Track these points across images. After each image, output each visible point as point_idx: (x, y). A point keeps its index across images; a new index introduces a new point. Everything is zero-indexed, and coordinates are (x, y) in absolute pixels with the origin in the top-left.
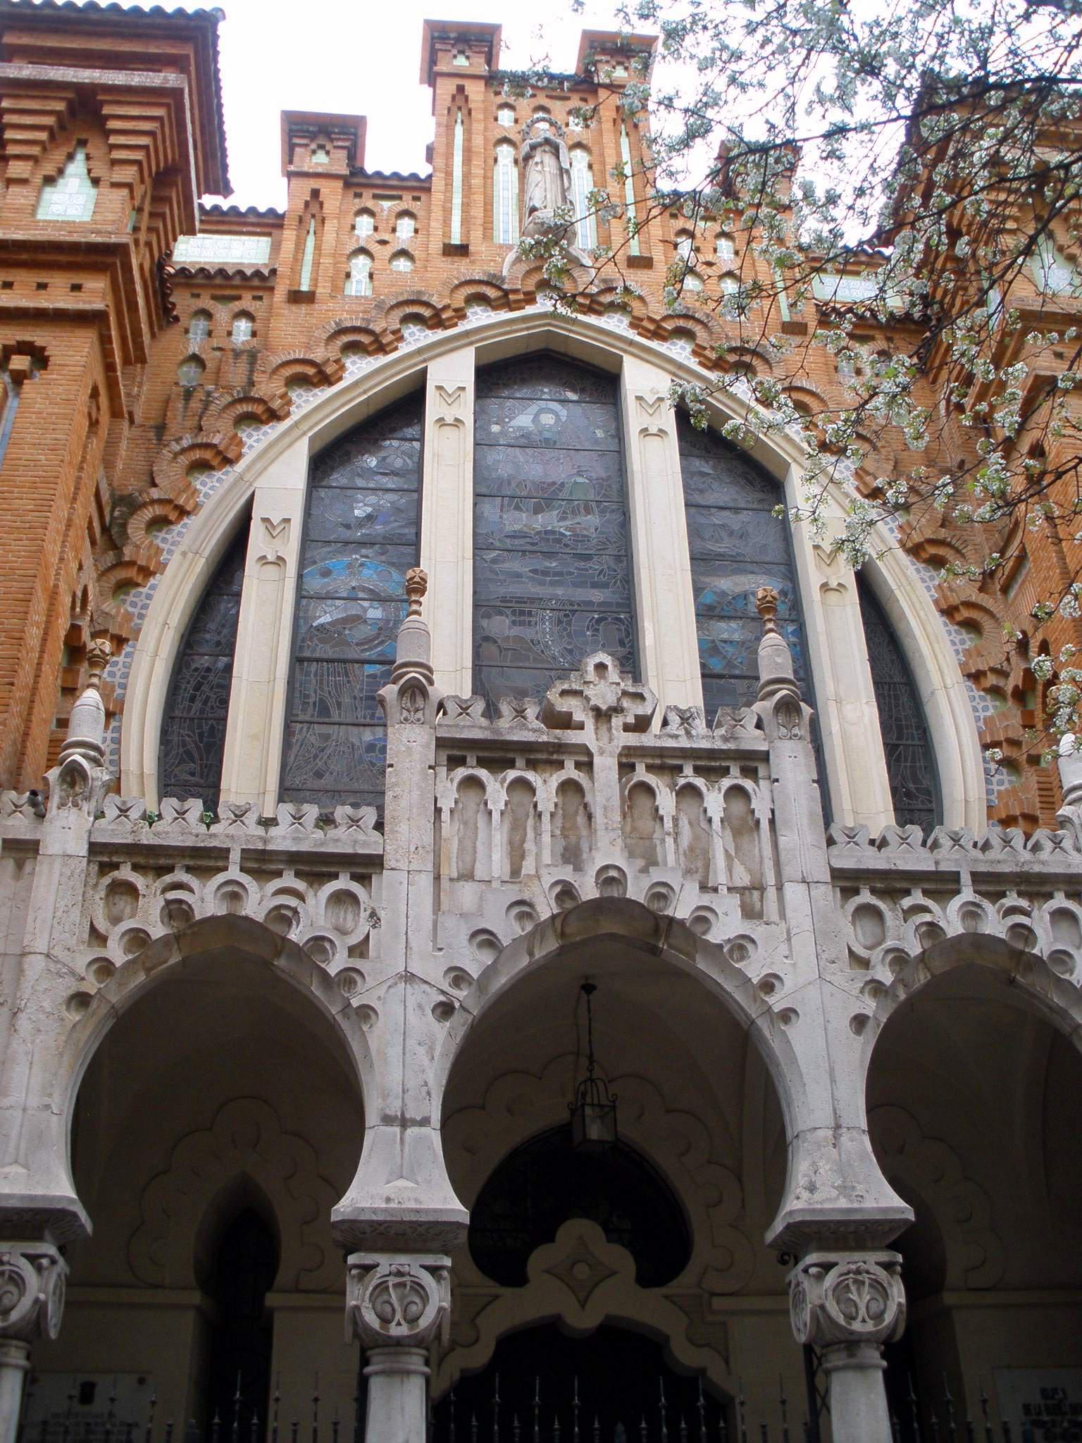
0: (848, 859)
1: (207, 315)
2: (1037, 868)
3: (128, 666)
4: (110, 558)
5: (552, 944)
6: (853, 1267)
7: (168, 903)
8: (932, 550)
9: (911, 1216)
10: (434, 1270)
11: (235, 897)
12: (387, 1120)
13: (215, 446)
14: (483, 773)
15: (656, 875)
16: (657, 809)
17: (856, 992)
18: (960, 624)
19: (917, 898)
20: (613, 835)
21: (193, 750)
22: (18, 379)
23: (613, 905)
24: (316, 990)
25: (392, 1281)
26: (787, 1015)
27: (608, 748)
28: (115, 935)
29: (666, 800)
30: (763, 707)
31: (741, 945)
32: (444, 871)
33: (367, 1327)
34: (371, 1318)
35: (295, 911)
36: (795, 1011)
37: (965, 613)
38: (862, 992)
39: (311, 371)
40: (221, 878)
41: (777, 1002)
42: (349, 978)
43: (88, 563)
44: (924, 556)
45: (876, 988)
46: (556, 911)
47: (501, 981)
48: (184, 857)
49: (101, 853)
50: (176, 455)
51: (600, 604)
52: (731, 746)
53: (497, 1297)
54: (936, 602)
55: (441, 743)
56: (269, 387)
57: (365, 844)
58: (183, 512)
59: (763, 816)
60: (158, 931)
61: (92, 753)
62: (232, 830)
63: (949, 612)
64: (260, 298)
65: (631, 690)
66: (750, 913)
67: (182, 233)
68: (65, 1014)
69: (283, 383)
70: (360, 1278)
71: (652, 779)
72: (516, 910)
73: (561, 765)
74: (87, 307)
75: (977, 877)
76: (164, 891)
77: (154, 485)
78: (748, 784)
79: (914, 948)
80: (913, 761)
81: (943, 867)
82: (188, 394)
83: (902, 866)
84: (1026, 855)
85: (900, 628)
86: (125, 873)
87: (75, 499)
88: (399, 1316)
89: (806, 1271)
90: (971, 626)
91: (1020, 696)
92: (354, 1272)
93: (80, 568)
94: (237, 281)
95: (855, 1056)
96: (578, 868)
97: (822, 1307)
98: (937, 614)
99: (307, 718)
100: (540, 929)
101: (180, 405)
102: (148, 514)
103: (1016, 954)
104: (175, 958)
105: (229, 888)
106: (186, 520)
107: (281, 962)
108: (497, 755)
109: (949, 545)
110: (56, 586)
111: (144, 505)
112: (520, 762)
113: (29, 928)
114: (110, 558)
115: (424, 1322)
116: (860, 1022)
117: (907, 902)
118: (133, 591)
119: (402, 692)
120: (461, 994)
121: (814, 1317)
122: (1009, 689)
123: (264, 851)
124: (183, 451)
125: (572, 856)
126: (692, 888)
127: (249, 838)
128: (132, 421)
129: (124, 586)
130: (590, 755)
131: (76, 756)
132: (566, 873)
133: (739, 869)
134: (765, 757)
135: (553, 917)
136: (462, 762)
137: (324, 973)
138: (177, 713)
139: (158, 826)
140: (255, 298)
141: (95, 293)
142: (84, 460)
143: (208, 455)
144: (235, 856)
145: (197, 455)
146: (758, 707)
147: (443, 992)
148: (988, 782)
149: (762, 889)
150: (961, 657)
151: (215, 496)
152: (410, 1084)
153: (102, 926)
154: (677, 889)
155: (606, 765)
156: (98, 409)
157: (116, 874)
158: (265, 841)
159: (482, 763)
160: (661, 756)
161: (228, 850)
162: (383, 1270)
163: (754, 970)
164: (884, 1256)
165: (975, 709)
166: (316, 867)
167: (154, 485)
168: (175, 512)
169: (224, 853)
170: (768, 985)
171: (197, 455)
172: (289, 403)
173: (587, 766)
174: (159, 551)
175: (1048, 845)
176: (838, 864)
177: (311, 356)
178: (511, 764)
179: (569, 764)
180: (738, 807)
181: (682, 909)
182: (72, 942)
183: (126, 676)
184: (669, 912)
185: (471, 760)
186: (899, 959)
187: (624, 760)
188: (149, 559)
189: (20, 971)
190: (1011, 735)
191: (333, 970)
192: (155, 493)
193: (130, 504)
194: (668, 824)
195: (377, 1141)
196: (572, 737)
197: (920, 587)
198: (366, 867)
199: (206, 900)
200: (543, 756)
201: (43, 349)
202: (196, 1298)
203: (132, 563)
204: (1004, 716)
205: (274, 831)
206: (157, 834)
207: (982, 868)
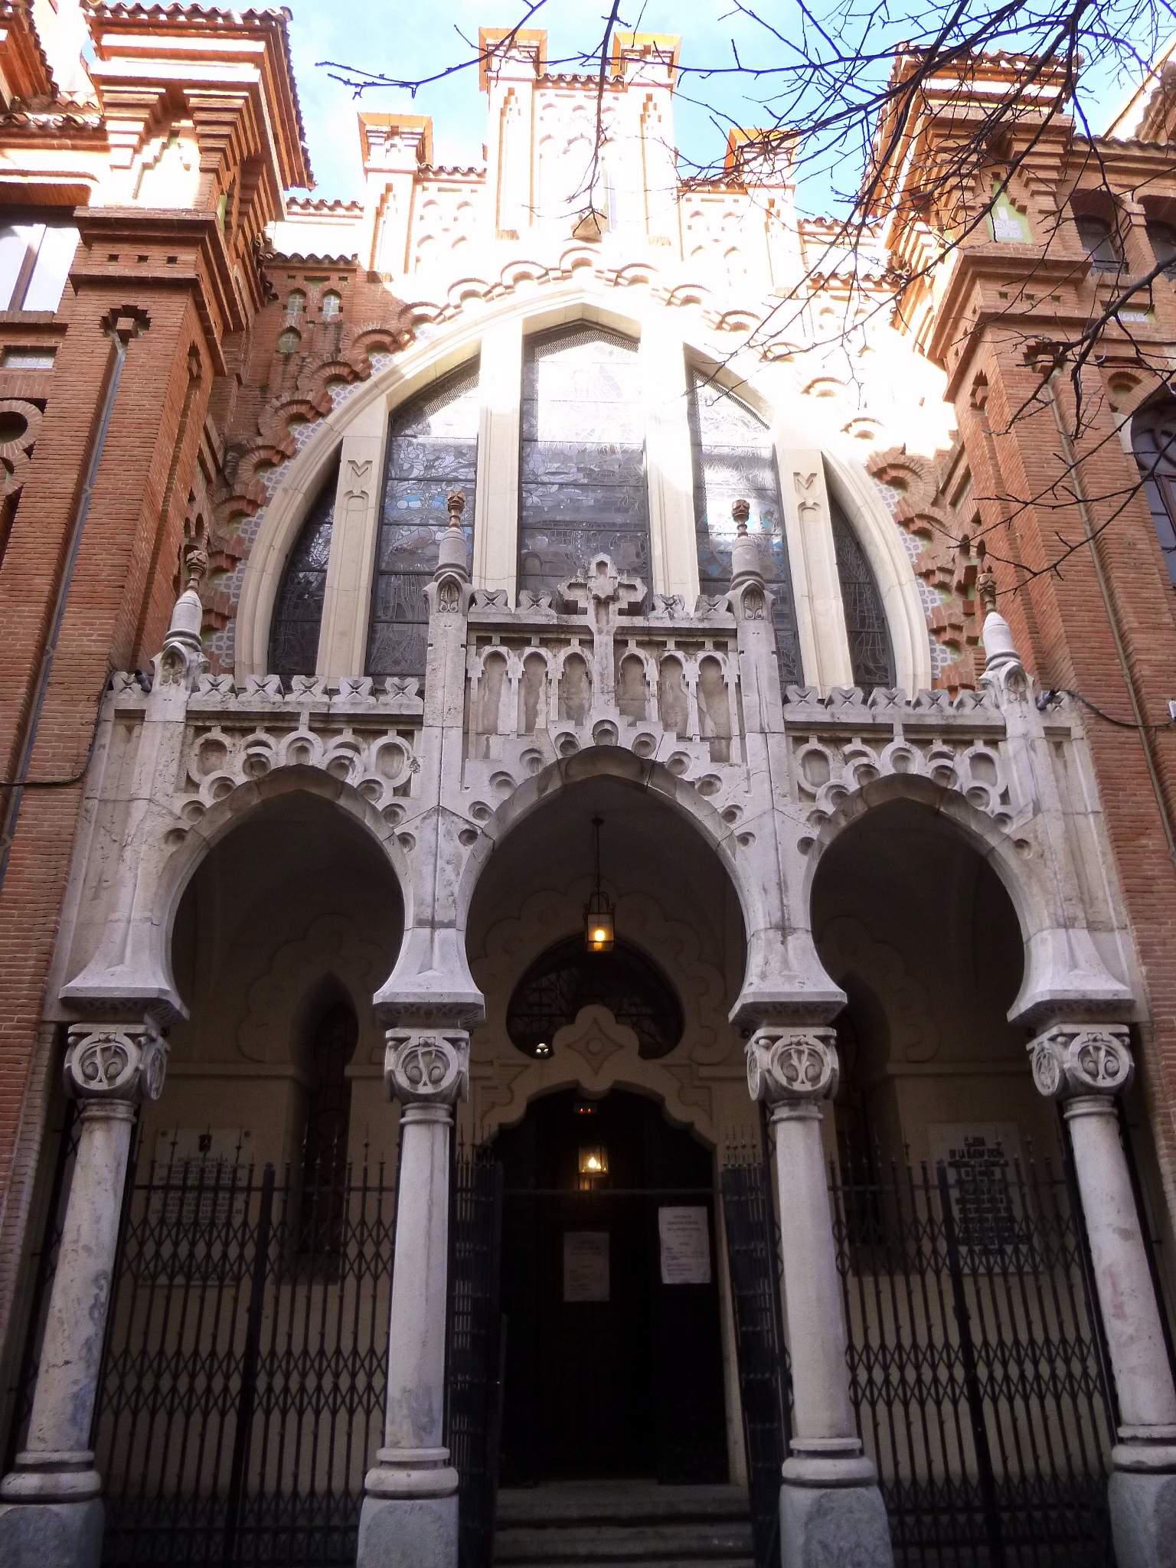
0: (800, 714)
1: (302, 293)
2: (959, 722)
3: (240, 580)
4: (224, 493)
5: (555, 785)
6: (795, 1040)
7: (250, 756)
8: (893, 473)
9: (845, 1000)
10: (454, 1042)
11: (303, 750)
12: (420, 923)
13: (307, 402)
14: (503, 650)
15: (642, 728)
16: (644, 676)
18: (915, 533)
19: (857, 745)
20: (607, 697)
21: (293, 645)
22: (125, 336)
23: (605, 752)
24: (368, 822)
25: (421, 1050)
26: (745, 839)
27: (604, 626)
28: (206, 782)
29: (651, 670)
30: (735, 594)
31: (709, 783)
32: (472, 727)
33: (401, 1088)
34: (402, 1080)
35: (351, 760)
36: (752, 835)
37: (919, 524)
38: (808, 820)
39: (387, 339)
40: (293, 735)
41: (738, 827)
42: (391, 813)
43: (201, 494)
45: (820, 817)
46: (560, 757)
47: (517, 812)
48: (263, 720)
49: (197, 719)
50: (277, 410)
51: (621, 525)
53: (527, 1066)
54: (895, 516)
55: (472, 627)
56: (352, 354)
57: (408, 706)
58: (284, 456)
59: (731, 679)
60: (240, 779)
61: (190, 641)
62: (302, 699)
63: (906, 523)
64: (345, 279)
65: (626, 582)
66: (718, 757)
67: (271, 219)
68: (163, 846)
69: (363, 350)
70: (396, 1048)
71: (641, 653)
72: (528, 757)
73: (568, 642)
74: (180, 276)
75: (908, 728)
76: (249, 746)
77: (260, 435)
79: (853, 786)
80: (873, 644)
81: (879, 720)
82: (287, 357)
83: (844, 719)
84: (950, 711)
85: (865, 538)
86: (216, 734)
87: (179, 440)
88: (425, 1078)
89: (757, 1042)
90: (924, 534)
91: (963, 589)
92: (390, 1043)
93: (192, 498)
94: (326, 265)
95: (801, 871)
96: (579, 723)
97: (769, 1071)
98: (896, 526)
99: (388, 618)
100: (548, 772)
101: (280, 369)
102: (255, 458)
103: (938, 788)
104: (256, 800)
105: (299, 744)
106: (286, 463)
107: (342, 802)
108: (516, 635)
109: (907, 468)
110: (165, 511)
111: (252, 450)
112: (535, 641)
113: (135, 779)
115: (446, 1083)
116: (806, 844)
117: (848, 749)
118: (244, 520)
119: (441, 587)
120: (482, 823)
121: (764, 1080)
122: (954, 584)
123: (328, 715)
124: (283, 406)
125: (573, 711)
126: (671, 737)
127: (316, 704)
128: (240, 382)
129: (238, 515)
130: (591, 633)
131: (176, 642)
132: (569, 727)
133: (709, 724)
134: (733, 633)
135: (559, 762)
136: (487, 641)
137: (374, 808)
138: (284, 617)
139: (242, 697)
140: (341, 279)
141: (188, 263)
142: (186, 407)
143: (303, 409)
144: (304, 718)
145: (295, 409)
146: (729, 595)
148: (933, 659)
150: (914, 559)
151: (310, 443)
152: (441, 893)
153: (196, 777)
154: (658, 739)
155: (604, 642)
156: (199, 366)
157: (208, 735)
158: (329, 707)
159: (504, 642)
160: (648, 635)
161: (299, 714)
162: (413, 1042)
163: (720, 801)
164: (821, 1031)
165: (924, 602)
166: (368, 726)
167: (260, 435)
168: (278, 455)
169: (294, 717)
170: (730, 814)
171: (295, 409)
172: (370, 366)
173: (588, 643)
174: (264, 488)
175: (970, 703)
176: (790, 718)
177: (386, 327)
178: (528, 642)
179: (575, 642)
180: (712, 673)
181: (662, 754)
182: (170, 790)
183: (239, 587)
184: (652, 757)
185: (496, 640)
186: (839, 793)
187: (619, 638)
188: (256, 494)
189: (128, 814)
190: (954, 621)
191: (380, 806)
192: (260, 441)
193: (242, 451)
194: (654, 688)
195: (412, 938)
196: (576, 620)
197: (882, 504)
199: (279, 753)
200: (553, 635)
201: (145, 312)
202: (290, 1070)
203: (242, 498)
204: (948, 606)
205: (336, 699)
206: (242, 703)
207: (913, 721)
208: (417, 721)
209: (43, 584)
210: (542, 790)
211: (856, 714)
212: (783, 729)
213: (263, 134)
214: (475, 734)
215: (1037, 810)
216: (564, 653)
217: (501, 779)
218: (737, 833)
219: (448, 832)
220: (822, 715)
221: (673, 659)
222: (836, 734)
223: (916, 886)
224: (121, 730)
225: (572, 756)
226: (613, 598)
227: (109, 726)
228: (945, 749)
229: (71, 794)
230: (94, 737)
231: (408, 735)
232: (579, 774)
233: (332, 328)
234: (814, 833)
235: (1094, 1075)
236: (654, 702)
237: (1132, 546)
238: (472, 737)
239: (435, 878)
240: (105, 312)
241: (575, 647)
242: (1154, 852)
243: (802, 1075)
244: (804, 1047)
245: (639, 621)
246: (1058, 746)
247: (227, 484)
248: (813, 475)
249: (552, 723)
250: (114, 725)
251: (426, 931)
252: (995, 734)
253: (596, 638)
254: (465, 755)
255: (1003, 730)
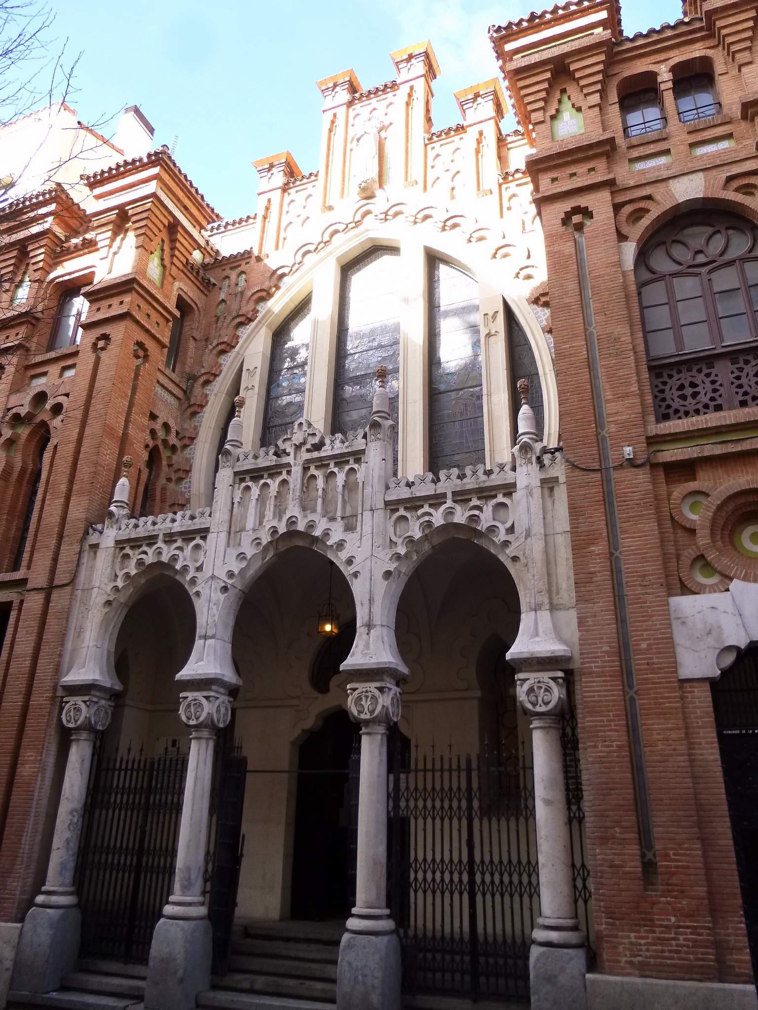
0: (392, 496)
1: (227, 277)
5: (271, 554)
11: (160, 553)
12: (201, 637)
14: (250, 484)
15: (311, 517)
17: (387, 559)
19: (426, 509)
25: (193, 703)
26: (356, 575)
29: (320, 483)
31: (341, 545)
32: (233, 529)
36: (358, 572)
38: (391, 559)
39: (264, 294)
42: (193, 581)
44: (541, 303)
45: (398, 557)
47: (251, 572)
50: (211, 351)
52: (349, 450)
55: (236, 474)
56: (247, 308)
58: (216, 376)
60: (133, 572)
62: (161, 527)
66: (349, 528)
75: (454, 494)
78: (356, 466)
83: (418, 494)
86: (128, 550)
100: (266, 548)
102: (201, 380)
103: (470, 528)
104: (143, 581)
111: (200, 377)
112: (266, 476)
114: (186, 405)
116: (388, 574)
117: (420, 512)
120: (230, 582)
124: (214, 348)
125: (279, 513)
128: (195, 339)
129: (194, 414)
132: (275, 523)
133: (348, 508)
134: (363, 452)
135: (271, 542)
144: (161, 537)
145: (220, 348)
147: (224, 582)
149: (356, 516)
151: (228, 363)
155: (297, 470)
163: (344, 555)
169: (156, 537)
170: (350, 562)
171: (220, 348)
173: (289, 472)
174: (207, 395)
178: (262, 477)
179: (284, 472)
181: (317, 533)
182: (106, 581)
185: (248, 479)
186: (410, 541)
192: (203, 371)
194: (320, 492)
198: (204, 533)
200: (273, 471)
203: (195, 404)
208: (207, 530)
209: (63, 488)
210: (263, 559)
211: (427, 489)
212: (382, 505)
213: (170, 213)
214: (233, 532)
215: (528, 535)
216: (279, 479)
217: (241, 556)
218: (351, 572)
219: (216, 589)
220: (405, 493)
221: (333, 473)
222: (413, 504)
223: (461, 590)
224: (92, 554)
225: (277, 539)
226: (304, 443)
227: (86, 554)
228: (478, 503)
229: (69, 588)
230: (79, 560)
231: (204, 538)
232: (282, 548)
233: (239, 295)
234: (392, 567)
235: (534, 705)
236: (320, 501)
237: (617, 340)
238: (232, 535)
239: (212, 611)
240: (93, 340)
241: (284, 476)
242: (599, 554)
243: (366, 710)
244: (369, 694)
245: (316, 454)
246: (551, 489)
247: (188, 399)
248: (497, 312)
249: (270, 521)
250: (89, 553)
251: (202, 641)
252: (509, 489)
253: (293, 469)
254: (228, 545)
255: (513, 485)
